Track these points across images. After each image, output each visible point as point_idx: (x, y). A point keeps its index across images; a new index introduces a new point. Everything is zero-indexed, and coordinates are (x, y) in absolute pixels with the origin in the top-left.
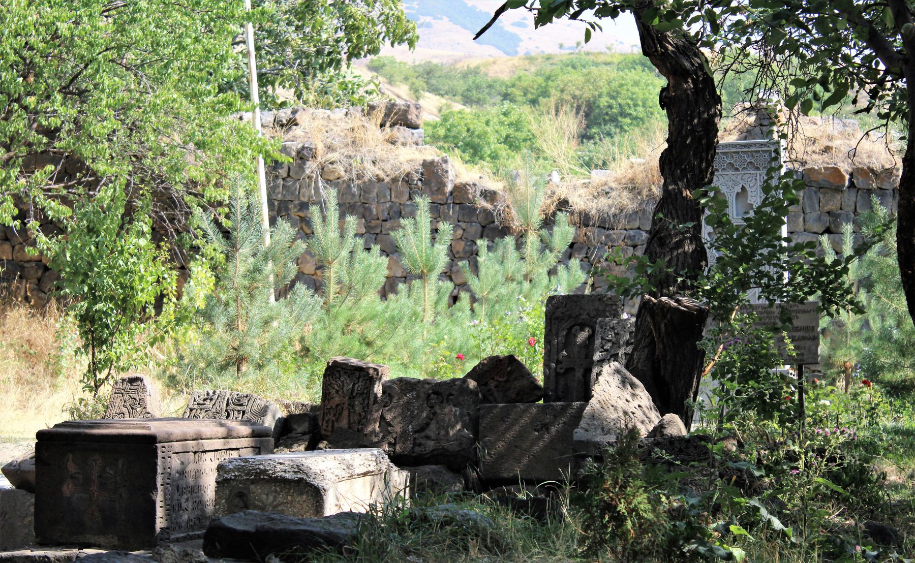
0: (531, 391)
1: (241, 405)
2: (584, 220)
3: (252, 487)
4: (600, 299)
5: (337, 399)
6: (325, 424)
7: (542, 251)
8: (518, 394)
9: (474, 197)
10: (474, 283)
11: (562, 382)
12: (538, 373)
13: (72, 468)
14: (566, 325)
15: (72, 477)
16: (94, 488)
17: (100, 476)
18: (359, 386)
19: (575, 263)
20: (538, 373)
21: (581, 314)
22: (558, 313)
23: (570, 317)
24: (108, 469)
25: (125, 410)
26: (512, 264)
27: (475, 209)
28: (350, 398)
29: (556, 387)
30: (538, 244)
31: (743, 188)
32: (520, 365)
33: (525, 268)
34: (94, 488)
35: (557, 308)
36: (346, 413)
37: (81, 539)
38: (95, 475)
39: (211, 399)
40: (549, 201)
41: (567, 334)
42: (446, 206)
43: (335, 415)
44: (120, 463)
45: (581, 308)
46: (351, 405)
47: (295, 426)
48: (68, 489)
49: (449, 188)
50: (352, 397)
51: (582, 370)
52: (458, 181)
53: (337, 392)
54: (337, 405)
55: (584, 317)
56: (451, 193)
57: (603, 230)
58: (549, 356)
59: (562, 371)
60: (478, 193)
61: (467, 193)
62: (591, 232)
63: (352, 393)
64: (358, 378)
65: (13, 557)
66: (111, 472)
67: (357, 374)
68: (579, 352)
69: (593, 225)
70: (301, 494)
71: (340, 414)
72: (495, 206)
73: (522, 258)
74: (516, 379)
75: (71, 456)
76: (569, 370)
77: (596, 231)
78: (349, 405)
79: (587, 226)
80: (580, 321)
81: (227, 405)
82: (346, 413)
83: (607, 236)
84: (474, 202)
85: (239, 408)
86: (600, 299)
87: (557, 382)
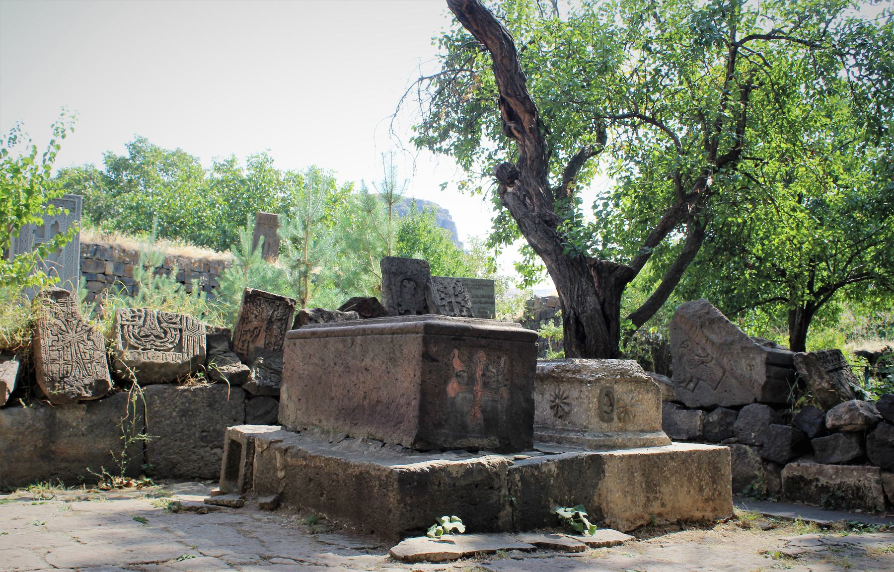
1: (175, 323)
3: (616, 386)
5: (255, 323)
6: (241, 344)
13: (457, 365)
14: (400, 278)
15: (457, 376)
16: (478, 388)
17: (484, 375)
18: (278, 313)
22: (394, 269)
23: (401, 273)
24: (490, 367)
25: (58, 322)
31: (56, 222)
34: (478, 388)
36: (263, 335)
37: (465, 443)
38: (479, 373)
39: (140, 317)
44: (503, 359)
46: (269, 329)
48: (453, 388)
53: (256, 316)
55: (409, 274)
65: (444, 469)
66: (494, 371)
67: (278, 303)
70: (648, 392)
71: (258, 335)
75: (456, 352)
81: (160, 322)
82: (263, 335)
85: (174, 326)
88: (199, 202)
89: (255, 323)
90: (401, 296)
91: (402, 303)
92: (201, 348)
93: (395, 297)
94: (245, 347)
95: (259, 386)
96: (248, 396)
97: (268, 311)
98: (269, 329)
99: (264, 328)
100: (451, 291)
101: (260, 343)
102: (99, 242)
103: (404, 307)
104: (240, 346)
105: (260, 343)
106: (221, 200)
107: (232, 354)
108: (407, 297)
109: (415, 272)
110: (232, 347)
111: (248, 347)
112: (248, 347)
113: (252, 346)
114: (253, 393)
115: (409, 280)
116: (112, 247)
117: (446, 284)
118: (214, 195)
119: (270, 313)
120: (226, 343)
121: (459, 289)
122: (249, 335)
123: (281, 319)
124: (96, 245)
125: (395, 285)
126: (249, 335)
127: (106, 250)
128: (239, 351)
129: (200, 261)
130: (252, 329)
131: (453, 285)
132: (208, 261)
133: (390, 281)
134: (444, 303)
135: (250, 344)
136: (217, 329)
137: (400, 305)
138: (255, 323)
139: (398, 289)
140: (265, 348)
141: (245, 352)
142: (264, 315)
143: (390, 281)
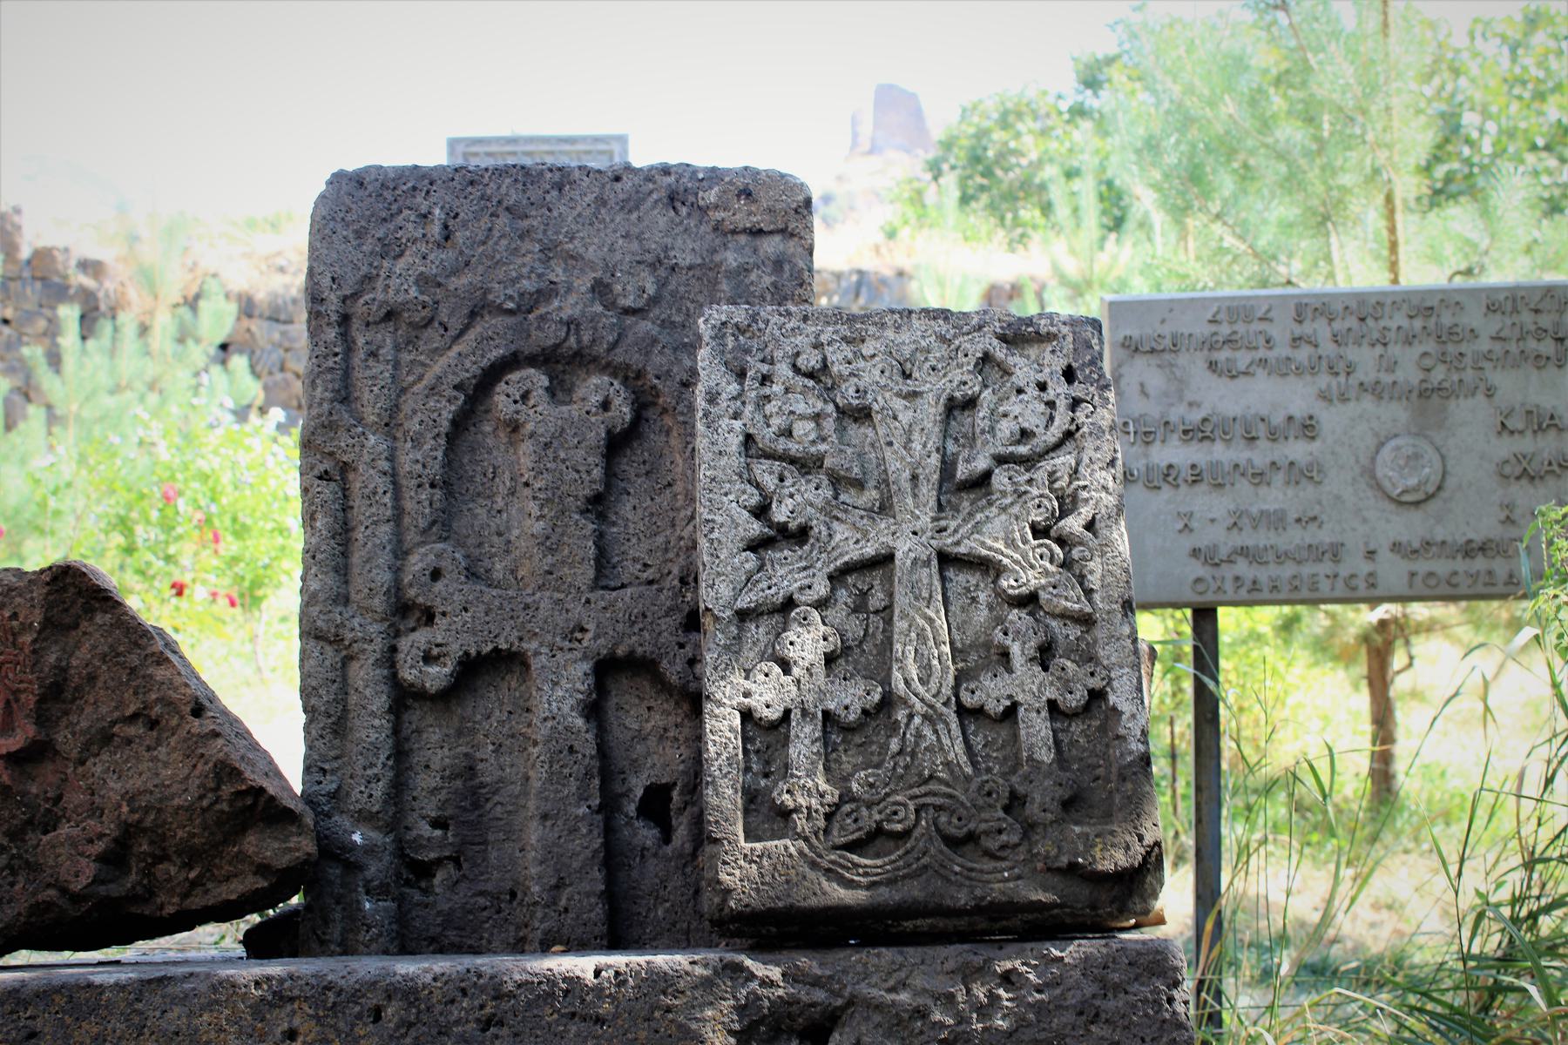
0: (215, 834)
2: (248, 308)
4: (673, 199)
7: (181, 340)
8: (115, 858)
9: (66, 268)
10: (46, 380)
11: (436, 751)
12: (256, 678)
14: (456, 361)
19: (239, 362)
20: (256, 678)
21: (547, 292)
22: (400, 282)
26: (130, 362)
27: (68, 287)
29: (399, 788)
30: (172, 330)
32: (141, 649)
33: (151, 369)
35: (391, 249)
40: (189, 277)
41: (461, 424)
42: (19, 283)
45: (548, 252)
49: (25, 253)
51: (577, 675)
52: (40, 244)
55: (567, 306)
56: (29, 262)
57: (275, 325)
58: (342, 570)
59: (436, 676)
60: (73, 263)
61: (53, 259)
62: (255, 326)
68: (549, 544)
69: (261, 316)
72: (101, 284)
73: (148, 353)
74: (106, 738)
76: (483, 669)
77: (266, 324)
79: (250, 316)
80: (549, 336)
83: (283, 334)
84: (66, 277)
86: (673, 199)
87: (400, 754)
90: (443, 524)
91: (449, 592)
93: (371, 537)
100: (909, 439)
102: (869, 263)
103: (456, 635)
108: (526, 521)
109: (633, 287)
115: (561, 365)
116: (901, 274)
117: (869, 376)
121: (1028, 412)
124: (860, 272)
125: (390, 424)
127: (883, 282)
131: (960, 378)
133: (345, 396)
134: (788, 574)
137: (406, 611)
139: (420, 457)
143: (345, 396)
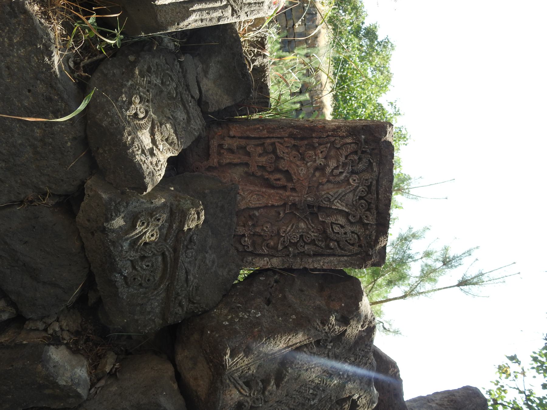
5: (301, 171)
6: (235, 144)
28: (310, 206)
36: (274, 198)
43: (263, 168)
46: (294, 210)
47: (214, 69)
50: (314, 210)
53: (321, 169)
54: (287, 173)
63: (320, 208)
64: (360, 221)
67: (371, 220)
71: (269, 185)
78: (294, 205)
82: (274, 198)
88: (361, 97)
89: (303, 171)
92: (181, 11)
94: (228, 158)
95: (104, 230)
96: (70, 203)
97: (340, 197)
98: (294, 210)
99: (295, 198)
101: (251, 197)
104: (228, 143)
105: (251, 197)
106: (368, 112)
107: (197, 124)
110: (219, 119)
111: (231, 165)
112: (231, 165)
113: (236, 174)
114: (81, 217)
118: (370, 108)
119: (338, 205)
120: (226, 102)
122: (263, 160)
123: (327, 238)
126: (263, 160)
128: (214, 143)
129: (322, 102)
130: (283, 165)
132: (323, 108)
135: (241, 170)
136: (261, 71)
138: (303, 171)
140: (239, 213)
141: (214, 161)
142: (328, 190)
